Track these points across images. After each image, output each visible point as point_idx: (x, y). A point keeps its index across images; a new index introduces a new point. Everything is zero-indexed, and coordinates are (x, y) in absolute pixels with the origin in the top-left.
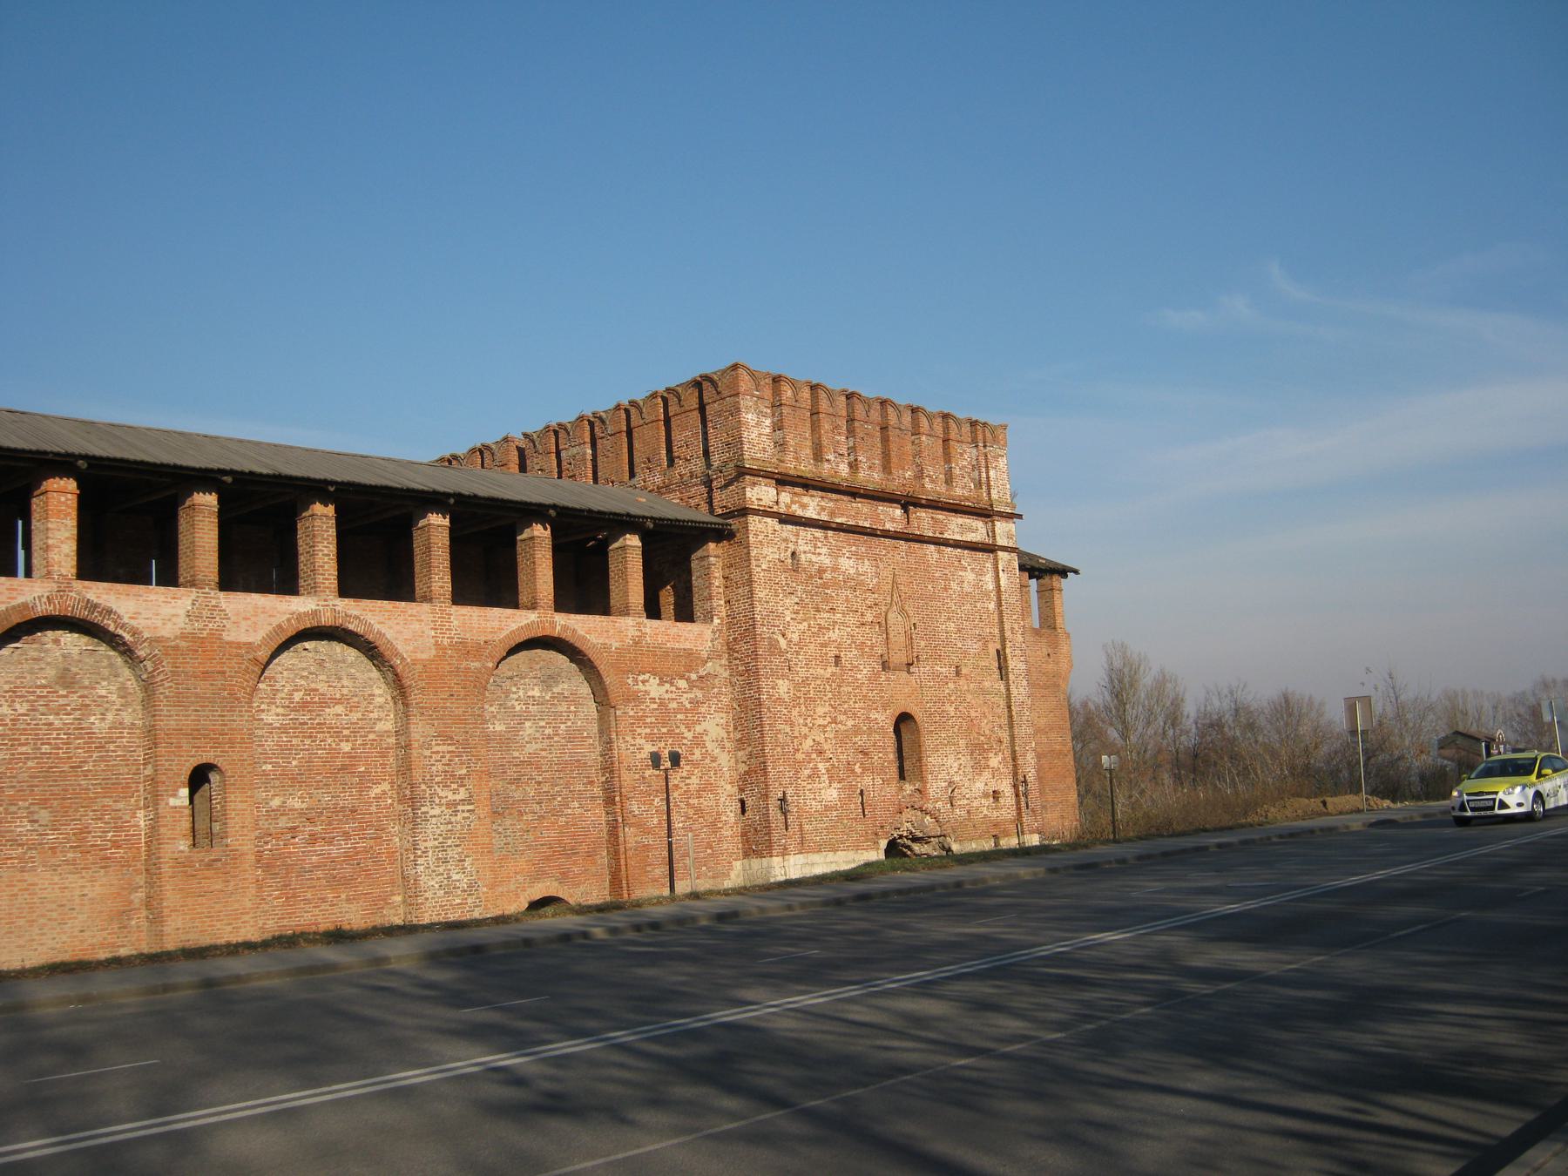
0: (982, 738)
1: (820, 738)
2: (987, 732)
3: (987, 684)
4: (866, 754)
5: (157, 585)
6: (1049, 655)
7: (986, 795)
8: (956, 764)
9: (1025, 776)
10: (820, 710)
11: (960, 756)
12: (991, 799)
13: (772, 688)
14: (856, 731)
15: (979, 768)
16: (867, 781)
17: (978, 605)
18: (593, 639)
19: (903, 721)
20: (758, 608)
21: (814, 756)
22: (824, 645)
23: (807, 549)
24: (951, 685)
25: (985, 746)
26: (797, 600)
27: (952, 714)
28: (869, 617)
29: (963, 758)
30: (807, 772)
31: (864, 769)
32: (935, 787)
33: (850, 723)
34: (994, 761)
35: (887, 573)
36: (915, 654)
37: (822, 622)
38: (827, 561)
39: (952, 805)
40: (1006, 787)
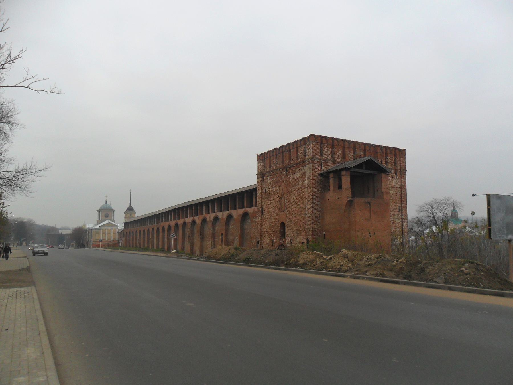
0: (300, 227)
1: (267, 228)
2: (301, 226)
3: (302, 212)
4: (274, 232)
5: (211, 213)
6: (338, 198)
7: (299, 243)
8: (293, 234)
9: (308, 238)
10: (267, 223)
11: (294, 232)
12: (301, 244)
13: (258, 219)
14: (273, 227)
15: (298, 235)
16: (274, 238)
17: (302, 190)
18: (250, 212)
19: (283, 225)
20: (257, 203)
21: (266, 232)
22: (269, 208)
23: (267, 188)
24: (293, 214)
25: (301, 230)
26: (265, 199)
27: (293, 221)
28: (277, 201)
29: (295, 233)
30: (264, 236)
31: (274, 235)
32: (288, 240)
33: (272, 225)
34: (303, 233)
35: (281, 189)
36: (286, 207)
37: (269, 203)
38: (271, 189)
39: (291, 245)
40: (305, 241)
